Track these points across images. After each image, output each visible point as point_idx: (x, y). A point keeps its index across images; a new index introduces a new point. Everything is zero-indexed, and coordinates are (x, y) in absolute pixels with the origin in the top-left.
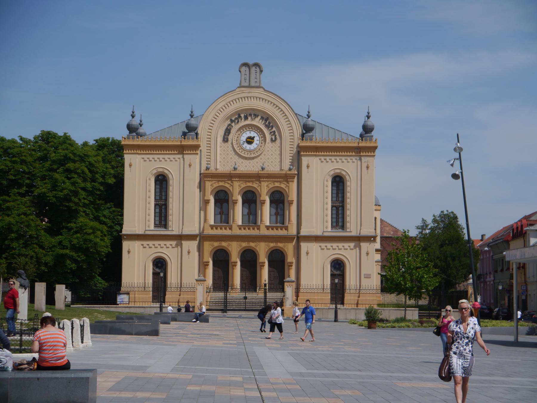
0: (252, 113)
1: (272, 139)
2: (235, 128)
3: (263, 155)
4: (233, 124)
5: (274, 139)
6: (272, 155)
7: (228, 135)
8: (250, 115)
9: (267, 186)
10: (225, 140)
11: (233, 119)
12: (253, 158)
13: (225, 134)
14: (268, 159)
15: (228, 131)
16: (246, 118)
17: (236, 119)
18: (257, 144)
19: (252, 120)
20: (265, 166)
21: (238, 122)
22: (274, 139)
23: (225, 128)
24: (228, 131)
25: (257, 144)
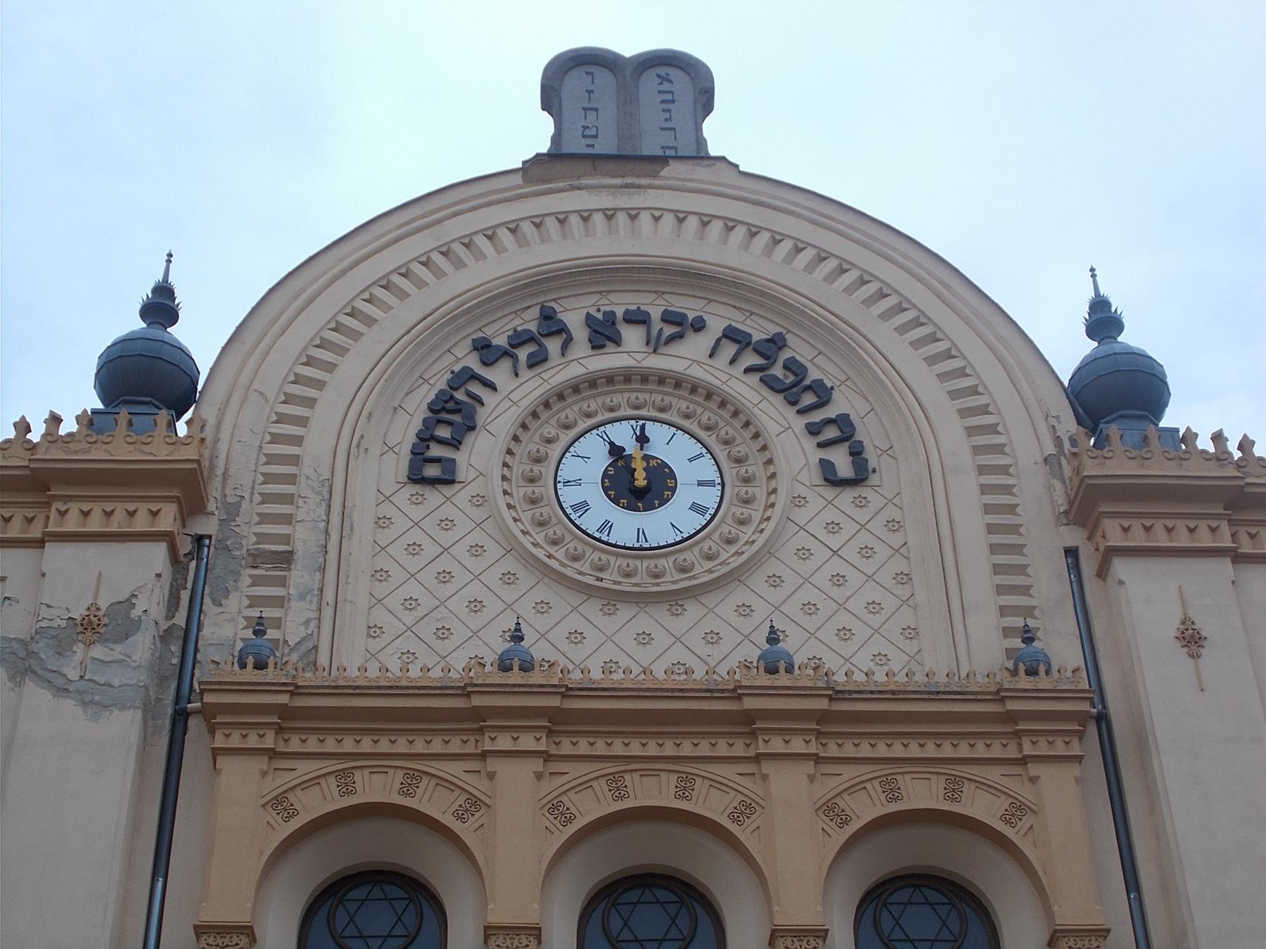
0: (655, 313)
1: (827, 468)
2: (509, 397)
3: (758, 581)
4: (499, 374)
5: (844, 467)
6: (838, 580)
7: (455, 444)
8: (638, 318)
9: (831, 810)
10: (429, 468)
11: (501, 341)
12: (674, 599)
13: (426, 437)
14: (810, 608)
15: (452, 415)
16: (603, 333)
17: (521, 338)
18: (697, 508)
19: (655, 344)
20: (797, 646)
21: (537, 361)
22: (844, 467)
23: (427, 394)
24: (452, 415)
25: (697, 508)
